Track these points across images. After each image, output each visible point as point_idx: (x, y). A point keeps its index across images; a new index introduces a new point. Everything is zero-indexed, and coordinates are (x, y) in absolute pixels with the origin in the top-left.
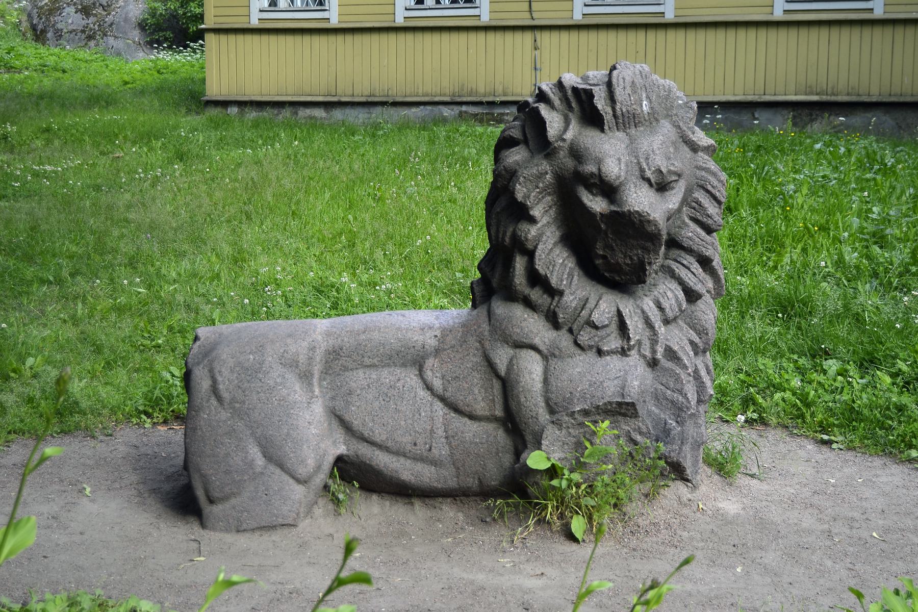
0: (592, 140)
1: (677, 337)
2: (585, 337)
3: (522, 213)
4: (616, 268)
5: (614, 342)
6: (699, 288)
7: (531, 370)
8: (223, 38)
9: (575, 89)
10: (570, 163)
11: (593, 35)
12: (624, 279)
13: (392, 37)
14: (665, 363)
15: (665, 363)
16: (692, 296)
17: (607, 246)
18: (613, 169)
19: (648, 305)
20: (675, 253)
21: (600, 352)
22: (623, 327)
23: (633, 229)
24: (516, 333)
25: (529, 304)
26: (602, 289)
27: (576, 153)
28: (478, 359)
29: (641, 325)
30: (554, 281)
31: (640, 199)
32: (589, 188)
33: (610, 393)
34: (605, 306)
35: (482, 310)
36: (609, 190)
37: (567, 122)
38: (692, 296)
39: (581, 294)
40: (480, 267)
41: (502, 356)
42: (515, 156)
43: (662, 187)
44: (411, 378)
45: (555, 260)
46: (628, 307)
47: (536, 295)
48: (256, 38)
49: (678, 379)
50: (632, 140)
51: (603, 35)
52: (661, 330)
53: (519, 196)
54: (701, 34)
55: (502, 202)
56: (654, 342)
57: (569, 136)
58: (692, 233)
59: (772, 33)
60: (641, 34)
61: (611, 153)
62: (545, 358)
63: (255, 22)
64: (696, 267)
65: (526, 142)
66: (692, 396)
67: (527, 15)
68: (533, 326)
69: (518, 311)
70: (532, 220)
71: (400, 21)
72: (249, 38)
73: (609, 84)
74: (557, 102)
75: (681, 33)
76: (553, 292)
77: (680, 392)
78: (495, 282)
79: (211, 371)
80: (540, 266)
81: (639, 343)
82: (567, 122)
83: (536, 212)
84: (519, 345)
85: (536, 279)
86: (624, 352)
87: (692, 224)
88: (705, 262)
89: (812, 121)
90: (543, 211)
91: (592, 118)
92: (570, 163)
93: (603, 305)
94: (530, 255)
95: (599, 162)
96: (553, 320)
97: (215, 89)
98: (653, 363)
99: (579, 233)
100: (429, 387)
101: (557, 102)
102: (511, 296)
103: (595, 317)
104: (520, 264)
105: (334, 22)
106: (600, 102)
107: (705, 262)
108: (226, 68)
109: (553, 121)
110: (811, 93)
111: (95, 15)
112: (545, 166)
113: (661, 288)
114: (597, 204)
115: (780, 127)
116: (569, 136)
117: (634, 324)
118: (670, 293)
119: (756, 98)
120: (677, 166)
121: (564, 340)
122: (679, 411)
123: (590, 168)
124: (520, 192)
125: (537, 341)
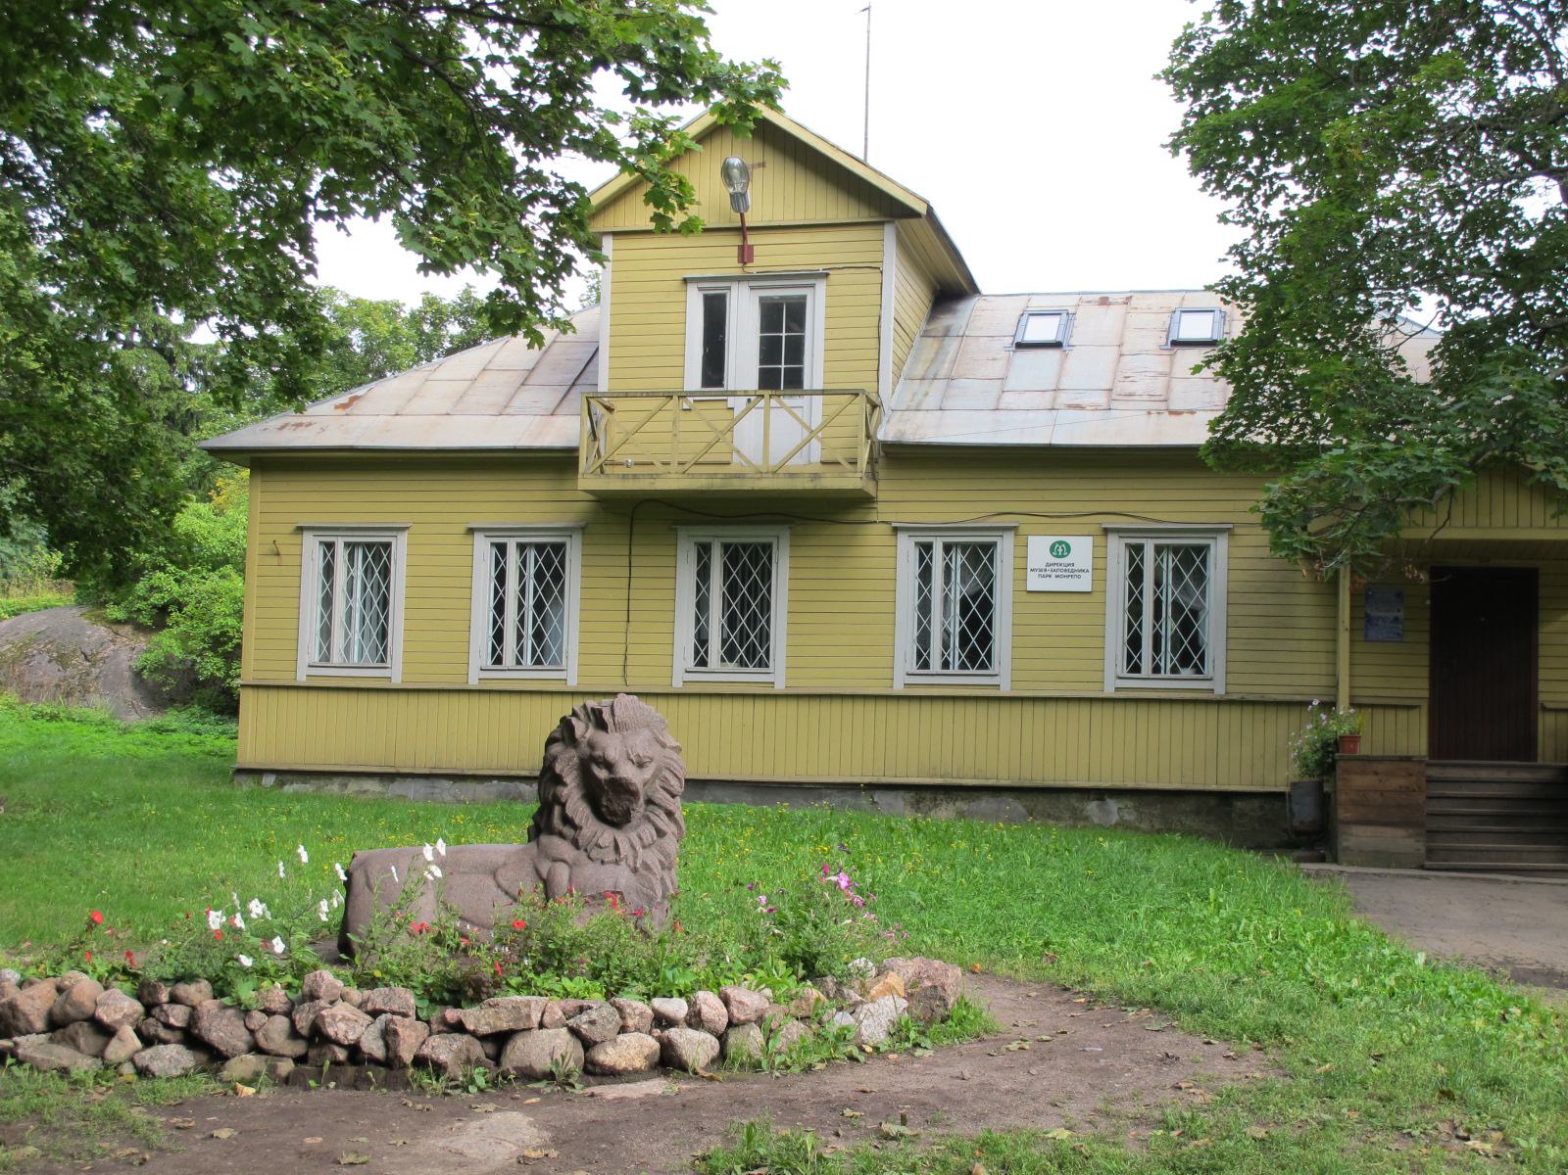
0: (601, 738)
1: (652, 857)
2: (593, 854)
3: (558, 780)
4: (614, 813)
5: (612, 856)
6: (664, 828)
7: (562, 873)
8: (263, 694)
9: (593, 709)
10: (587, 751)
11: (694, 703)
12: (616, 819)
13: (464, 698)
14: (642, 871)
15: (642, 871)
16: (660, 833)
17: (609, 800)
18: (612, 754)
19: (633, 836)
20: (651, 807)
21: (603, 862)
22: (617, 848)
23: (622, 788)
24: (555, 853)
25: (561, 835)
26: (605, 826)
27: (591, 745)
28: (530, 869)
29: (627, 846)
30: (577, 821)
31: (627, 771)
32: (598, 764)
33: (609, 885)
34: (607, 835)
35: (533, 844)
36: (609, 766)
37: (587, 728)
38: (660, 833)
39: (594, 829)
40: (534, 818)
41: (544, 869)
42: (556, 748)
43: (641, 765)
44: (490, 882)
45: (577, 807)
46: (620, 836)
47: (568, 831)
48: (303, 696)
49: (650, 882)
50: (624, 737)
51: (706, 703)
52: (640, 850)
53: (558, 770)
54: (815, 705)
55: (549, 775)
56: (636, 857)
57: (588, 735)
58: (661, 796)
59: (892, 707)
60: (749, 703)
61: (612, 746)
62: (570, 867)
63: (302, 679)
64: (663, 816)
65: (563, 740)
66: (660, 894)
67: (621, 681)
68: (563, 848)
69: (556, 840)
70: (565, 784)
71: (473, 682)
72: (293, 694)
73: (612, 707)
74: (582, 716)
75: (792, 705)
76: (576, 828)
77: (652, 889)
78: (542, 825)
79: (366, 872)
80: (569, 812)
81: (626, 857)
82: (587, 728)
83: (568, 780)
84: (555, 860)
85: (567, 821)
86: (617, 862)
87: (662, 791)
88: (670, 814)
89: (936, 806)
90: (571, 779)
91: (601, 725)
92: (587, 751)
93: (606, 835)
94: (563, 805)
95: (604, 749)
96: (575, 844)
97: (248, 757)
98: (635, 870)
99: (593, 793)
100: (499, 886)
101: (582, 716)
102: (551, 831)
103: (600, 842)
104: (557, 810)
105: (397, 681)
106: (606, 716)
107: (670, 814)
108: (266, 732)
109: (579, 727)
110: (935, 776)
111: (74, 666)
112: (573, 752)
113: (642, 828)
114: (602, 774)
115: (901, 813)
116: (588, 735)
117: (624, 847)
118: (648, 832)
119: (874, 780)
120: (650, 753)
121: (582, 855)
122: (650, 900)
123: (598, 753)
124: (558, 768)
125: (566, 857)
